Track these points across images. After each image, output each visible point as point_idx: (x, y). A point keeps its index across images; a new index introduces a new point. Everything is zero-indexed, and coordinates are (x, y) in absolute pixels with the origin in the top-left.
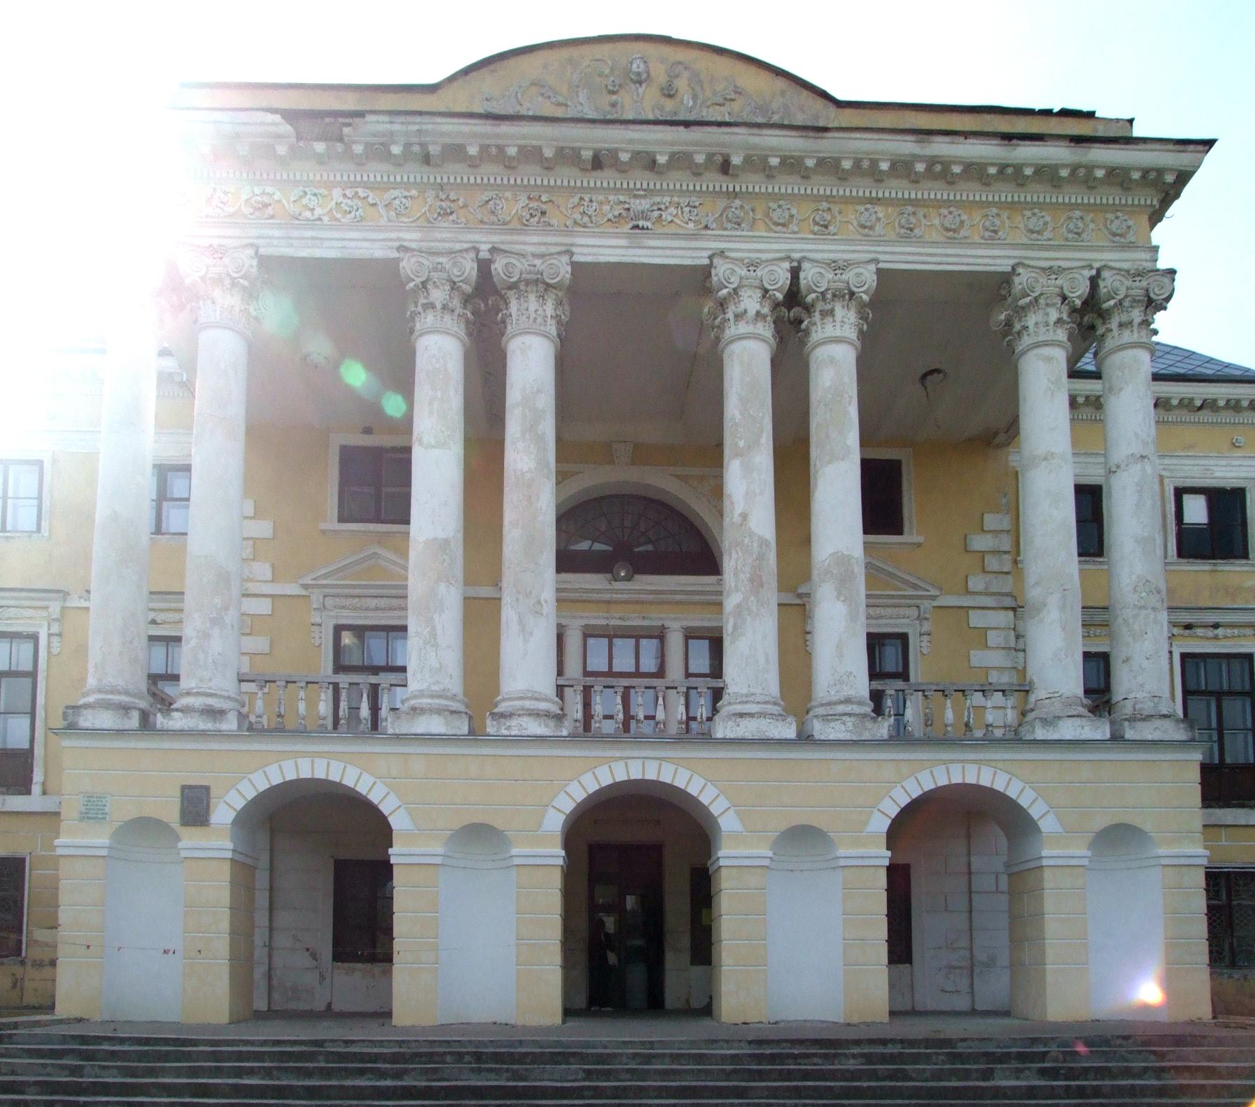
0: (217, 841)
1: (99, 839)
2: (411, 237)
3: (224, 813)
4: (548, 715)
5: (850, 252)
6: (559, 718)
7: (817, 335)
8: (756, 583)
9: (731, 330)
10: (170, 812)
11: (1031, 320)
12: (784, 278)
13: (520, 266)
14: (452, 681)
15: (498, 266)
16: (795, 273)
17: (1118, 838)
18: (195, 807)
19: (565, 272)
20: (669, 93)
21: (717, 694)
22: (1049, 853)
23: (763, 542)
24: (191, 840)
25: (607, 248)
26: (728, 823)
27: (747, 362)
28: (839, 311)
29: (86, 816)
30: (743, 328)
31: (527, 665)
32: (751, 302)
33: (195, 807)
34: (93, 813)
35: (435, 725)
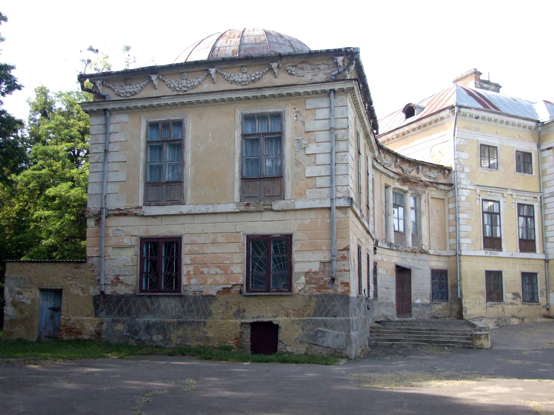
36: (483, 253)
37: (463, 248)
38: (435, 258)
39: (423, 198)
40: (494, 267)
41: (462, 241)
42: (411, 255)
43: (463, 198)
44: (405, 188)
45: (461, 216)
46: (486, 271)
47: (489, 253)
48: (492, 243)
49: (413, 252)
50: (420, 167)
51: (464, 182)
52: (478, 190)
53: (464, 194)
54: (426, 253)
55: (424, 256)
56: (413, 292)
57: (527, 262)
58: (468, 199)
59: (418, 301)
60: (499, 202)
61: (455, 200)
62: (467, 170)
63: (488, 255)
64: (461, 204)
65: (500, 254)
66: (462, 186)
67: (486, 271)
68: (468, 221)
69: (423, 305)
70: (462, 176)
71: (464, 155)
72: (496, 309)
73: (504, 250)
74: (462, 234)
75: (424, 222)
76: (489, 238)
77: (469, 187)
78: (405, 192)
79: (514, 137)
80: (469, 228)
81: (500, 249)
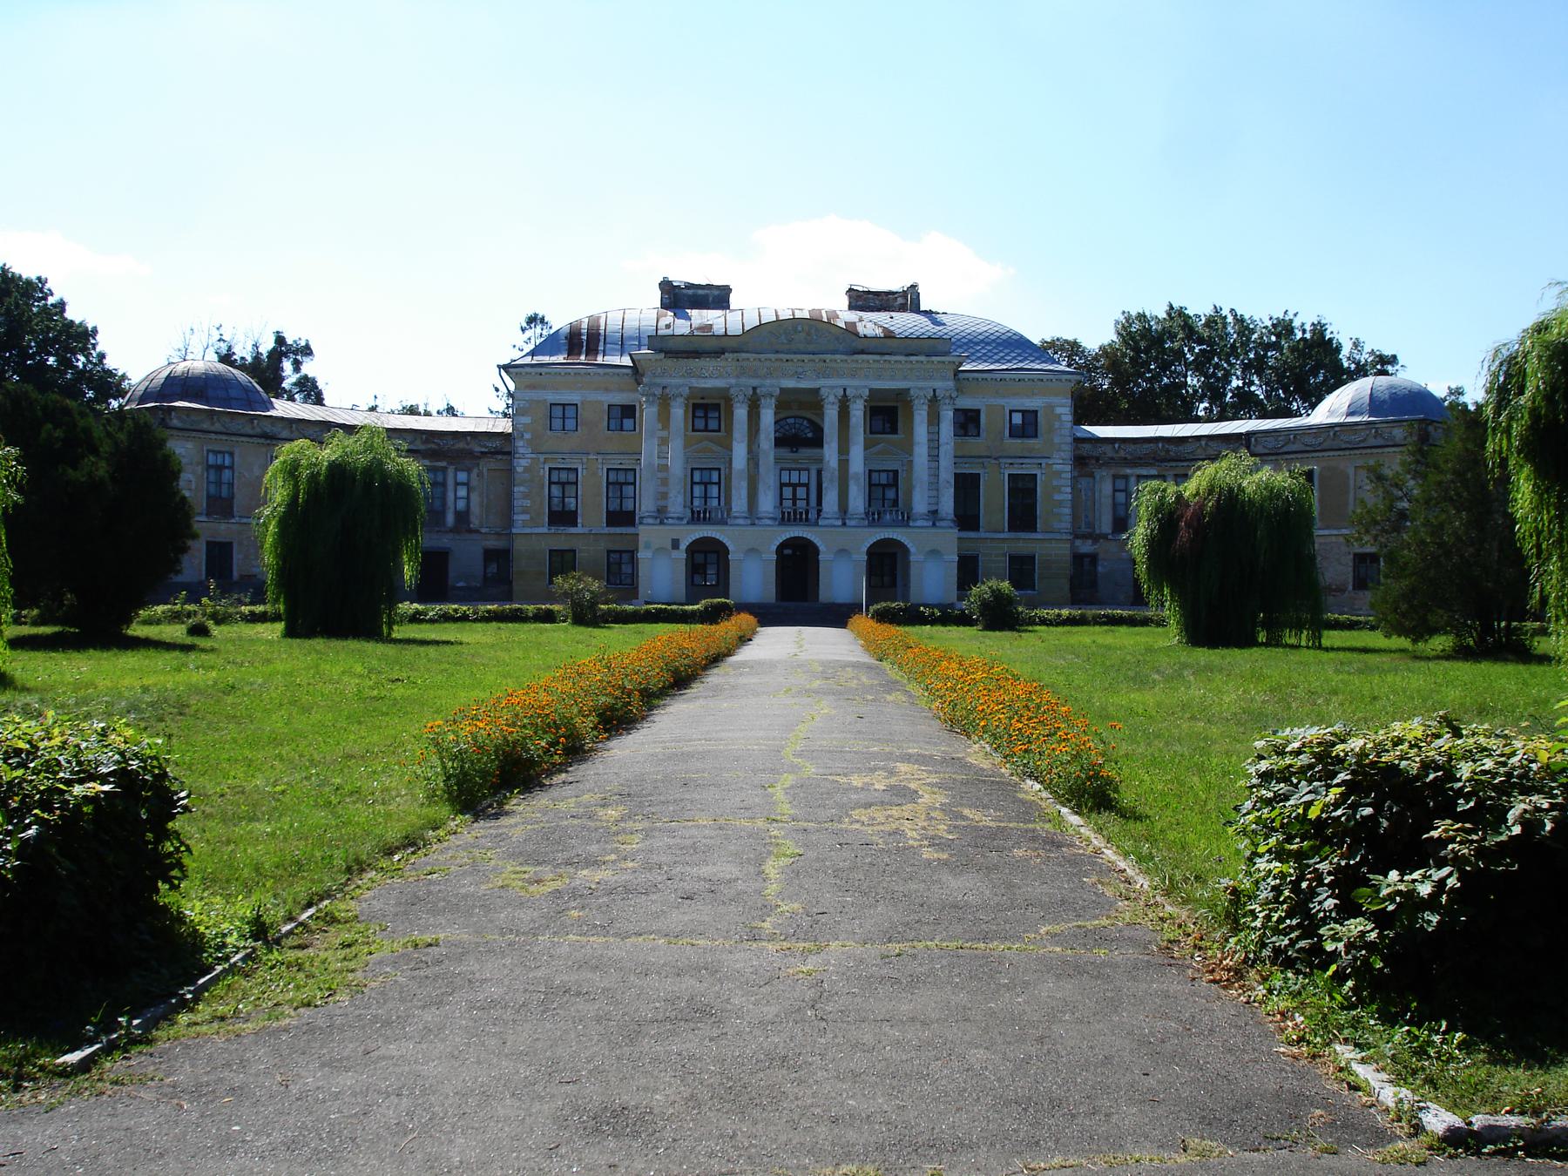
0: (681, 554)
2: (733, 381)
3: (683, 546)
5: (861, 381)
14: (745, 508)
17: (934, 553)
18: (675, 544)
19: (778, 391)
21: (819, 512)
22: (912, 558)
24: (675, 554)
25: (790, 383)
26: (822, 548)
27: (831, 415)
31: (767, 503)
32: (832, 399)
33: (675, 544)
34: (647, 546)
35: (741, 521)
39: (475, 471)
40: (562, 544)
42: (451, 536)
43: (519, 469)
44: (444, 464)
48: (562, 517)
49: (453, 530)
51: (521, 450)
52: (542, 458)
53: (521, 464)
54: (477, 531)
55: (474, 536)
56: (452, 574)
58: (527, 469)
59: (461, 584)
61: (510, 471)
62: (527, 436)
65: (572, 530)
68: (526, 496)
71: (526, 420)
75: (475, 497)
78: (444, 470)
80: (528, 503)
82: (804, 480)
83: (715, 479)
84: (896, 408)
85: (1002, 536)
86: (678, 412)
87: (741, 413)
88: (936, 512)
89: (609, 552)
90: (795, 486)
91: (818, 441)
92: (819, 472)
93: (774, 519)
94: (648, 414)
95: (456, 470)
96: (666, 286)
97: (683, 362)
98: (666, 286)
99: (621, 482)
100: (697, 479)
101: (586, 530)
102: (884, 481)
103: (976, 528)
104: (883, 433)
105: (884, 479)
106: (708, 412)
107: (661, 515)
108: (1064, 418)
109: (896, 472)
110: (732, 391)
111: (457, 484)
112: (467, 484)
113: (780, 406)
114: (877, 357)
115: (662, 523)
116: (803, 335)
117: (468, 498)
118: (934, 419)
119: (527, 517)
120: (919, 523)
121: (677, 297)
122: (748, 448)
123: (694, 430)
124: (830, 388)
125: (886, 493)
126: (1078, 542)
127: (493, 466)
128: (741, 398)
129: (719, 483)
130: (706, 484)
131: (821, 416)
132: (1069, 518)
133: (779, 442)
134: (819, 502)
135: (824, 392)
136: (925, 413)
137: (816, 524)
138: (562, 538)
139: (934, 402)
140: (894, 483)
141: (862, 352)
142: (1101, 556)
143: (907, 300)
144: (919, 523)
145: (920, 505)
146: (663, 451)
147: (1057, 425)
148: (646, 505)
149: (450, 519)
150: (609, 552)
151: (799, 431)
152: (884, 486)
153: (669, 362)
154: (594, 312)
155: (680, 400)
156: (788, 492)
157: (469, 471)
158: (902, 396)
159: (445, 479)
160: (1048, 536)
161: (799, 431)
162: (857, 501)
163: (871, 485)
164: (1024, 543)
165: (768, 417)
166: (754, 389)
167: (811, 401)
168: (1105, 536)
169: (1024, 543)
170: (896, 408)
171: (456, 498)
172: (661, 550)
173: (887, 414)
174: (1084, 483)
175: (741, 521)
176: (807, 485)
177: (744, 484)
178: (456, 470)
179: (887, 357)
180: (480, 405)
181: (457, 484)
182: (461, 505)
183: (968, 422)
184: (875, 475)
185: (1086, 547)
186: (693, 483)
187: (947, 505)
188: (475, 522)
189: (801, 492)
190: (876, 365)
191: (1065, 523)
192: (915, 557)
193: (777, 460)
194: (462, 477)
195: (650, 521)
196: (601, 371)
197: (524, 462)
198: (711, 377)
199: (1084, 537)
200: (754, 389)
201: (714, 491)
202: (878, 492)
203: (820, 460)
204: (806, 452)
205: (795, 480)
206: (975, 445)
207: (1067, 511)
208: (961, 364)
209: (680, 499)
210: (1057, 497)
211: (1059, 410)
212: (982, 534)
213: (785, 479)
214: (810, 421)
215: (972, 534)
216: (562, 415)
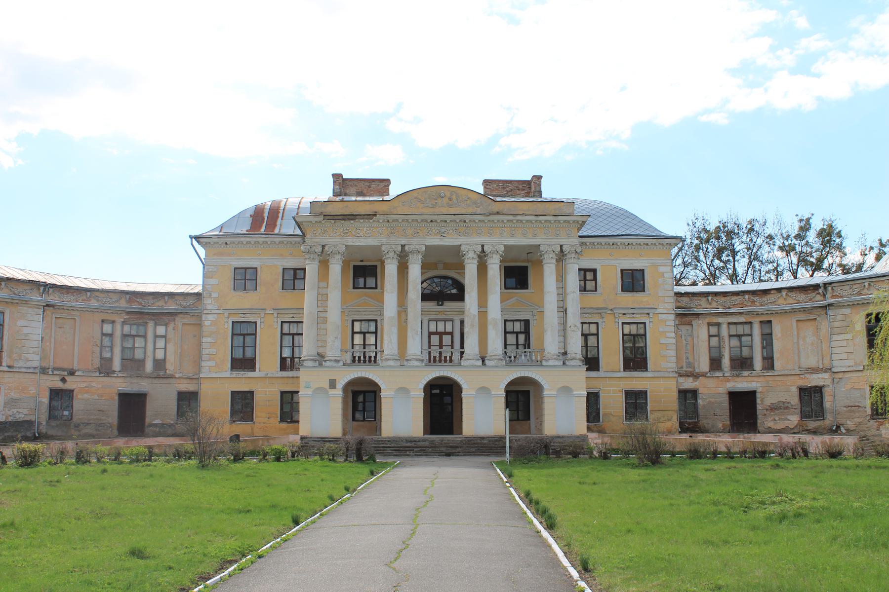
0: (338, 392)
1: (309, 392)
2: (384, 240)
3: (340, 385)
4: (419, 360)
5: (498, 241)
6: (422, 361)
7: (489, 262)
8: (472, 326)
9: (466, 261)
10: (327, 386)
11: (546, 256)
12: (480, 249)
13: (412, 247)
14: (395, 350)
15: (406, 248)
16: (483, 246)
17: (566, 390)
18: (333, 384)
19: (424, 248)
20: (450, 199)
21: (462, 353)
22: (545, 393)
23: (474, 316)
24: (332, 392)
25: (435, 241)
26: (464, 386)
28: (494, 256)
29: (306, 387)
30: (469, 261)
31: (415, 346)
32: (471, 254)
33: (333, 384)
34: (307, 386)
35: (392, 363)
36: (228, 374)
37: (203, 370)
38: (185, 381)
39: (171, 325)
41: (203, 364)
43: (207, 323)
45: (204, 340)
46: (232, 392)
47: (235, 374)
50: (166, 298)
51: (209, 307)
52: (226, 313)
53: (208, 320)
56: (149, 413)
57: (291, 381)
60: (255, 323)
61: (200, 325)
62: (214, 295)
63: (234, 375)
64: (204, 329)
65: (251, 374)
66: (205, 312)
67: (232, 392)
69: (163, 425)
70: (209, 301)
72: (240, 428)
73: (257, 370)
74: (204, 358)
75: (170, 347)
76: (239, 359)
77: (214, 312)
79: (282, 255)
80: (213, 351)
81: (253, 368)
82: (449, 329)
83: (373, 329)
84: (526, 268)
85: (619, 375)
86: (336, 269)
87: (391, 269)
88: (565, 353)
89: (282, 393)
90: (441, 334)
91: (460, 296)
92: (462, 322)
93: (422, 361)
94: (312, 270)
95: (156, 324)
96: (337, 177)
97: (339, 223)
98: (337, 177)
99: (291, 333)
100: (357, 327)
101: (262, 374)
102: (517, 329)
103: (598, 370)
104: (516, 288)
105: (517, 327)
106: (364, 273)
107: (320, 358)
108: (666, 275)
109: (527, 323)
110: (383, 248)
111: (156, 336)
112: (165, 337)
113: (425, 267)
114: (511, 218)
115: (320, 365)
116: (446, 200)
117: (165, 348)
118: (561, 277)
119: (212, 363)
120: (551, 363)
121: (341, 183)
122: (399, 301)
123: (354, 288)
124: (470, 245)
125: (521, 334)
126: (681, 380)
127: (186, 321)
128: (391, 254)
129: (376, 333)
130: (364, 333)
131: (463, 274)
132: (674, 359)
133: (425, 297)
134: (462, 346)
135: (463, 248)
136: (553, 267)
137: (460, 364)
138: (243, 382)
139: (561, 256)
140: (527, 332)
141: (498, 213)
142: (701, 391)
143: (531, 187)
144: (551, 363)
145: (551, 344)
146: (326, 303)
147: (661, 281)
148: (307, 348)
149: (149, 366)
150: (282, 393)
151: (444, 290)
152: (517, 333)
153: (328, 224)
154: (277, 198)
155: (338, 257)
156: (435, 339)
157: (166, 325)
158: (534, 254)
159: (146, 333)
160: (656, 375)
161: (444, 290)
162: (495, 344)
163: (506, 333)
164: (637, 381)
165: (415, 272)
166: (403, 246)
167: (455, 257)
168: (704, 375)
169: (637, 381)
170: (526, 268)
171: (155, 349)
172: (320, 390)
173: (517, 276)
174: (684, 329)
175: (392, 363)
176: (451, 334)
177: (395, 330)
178: (156, 324)
179: (519, 218)
180: (179, 271)
181: (156, 336)
182: (160, 355)
183: (588, 276)
184: (509, 324)
185: (688, 384)
186: (353, 333)
187: (576, 347)
188: (170, 368)
189: (447, 339)
190: (509, 224)
191: (672, 365)
192: (549, 392)
193: (424, 312)
194: (161, 330)
195: (310, 364)
196: (277, 240)
197: (211, 317)
198: (365, 238)
199: (687, 375)
200: (403, 246)
201: (371, 339)
202: (511, 339)
203: (462, 312)
204: (449, 305)
205: (441, 329)
206: (594, 300)
207: (673, 353)
208: (584, 222)
209: (338, 344)
210: (663, 341)
211: (662, 269)
212: (601, 373)
213: (433, 329)
214: (453, 280)
215: (593, 374)
216: (245, 278)
